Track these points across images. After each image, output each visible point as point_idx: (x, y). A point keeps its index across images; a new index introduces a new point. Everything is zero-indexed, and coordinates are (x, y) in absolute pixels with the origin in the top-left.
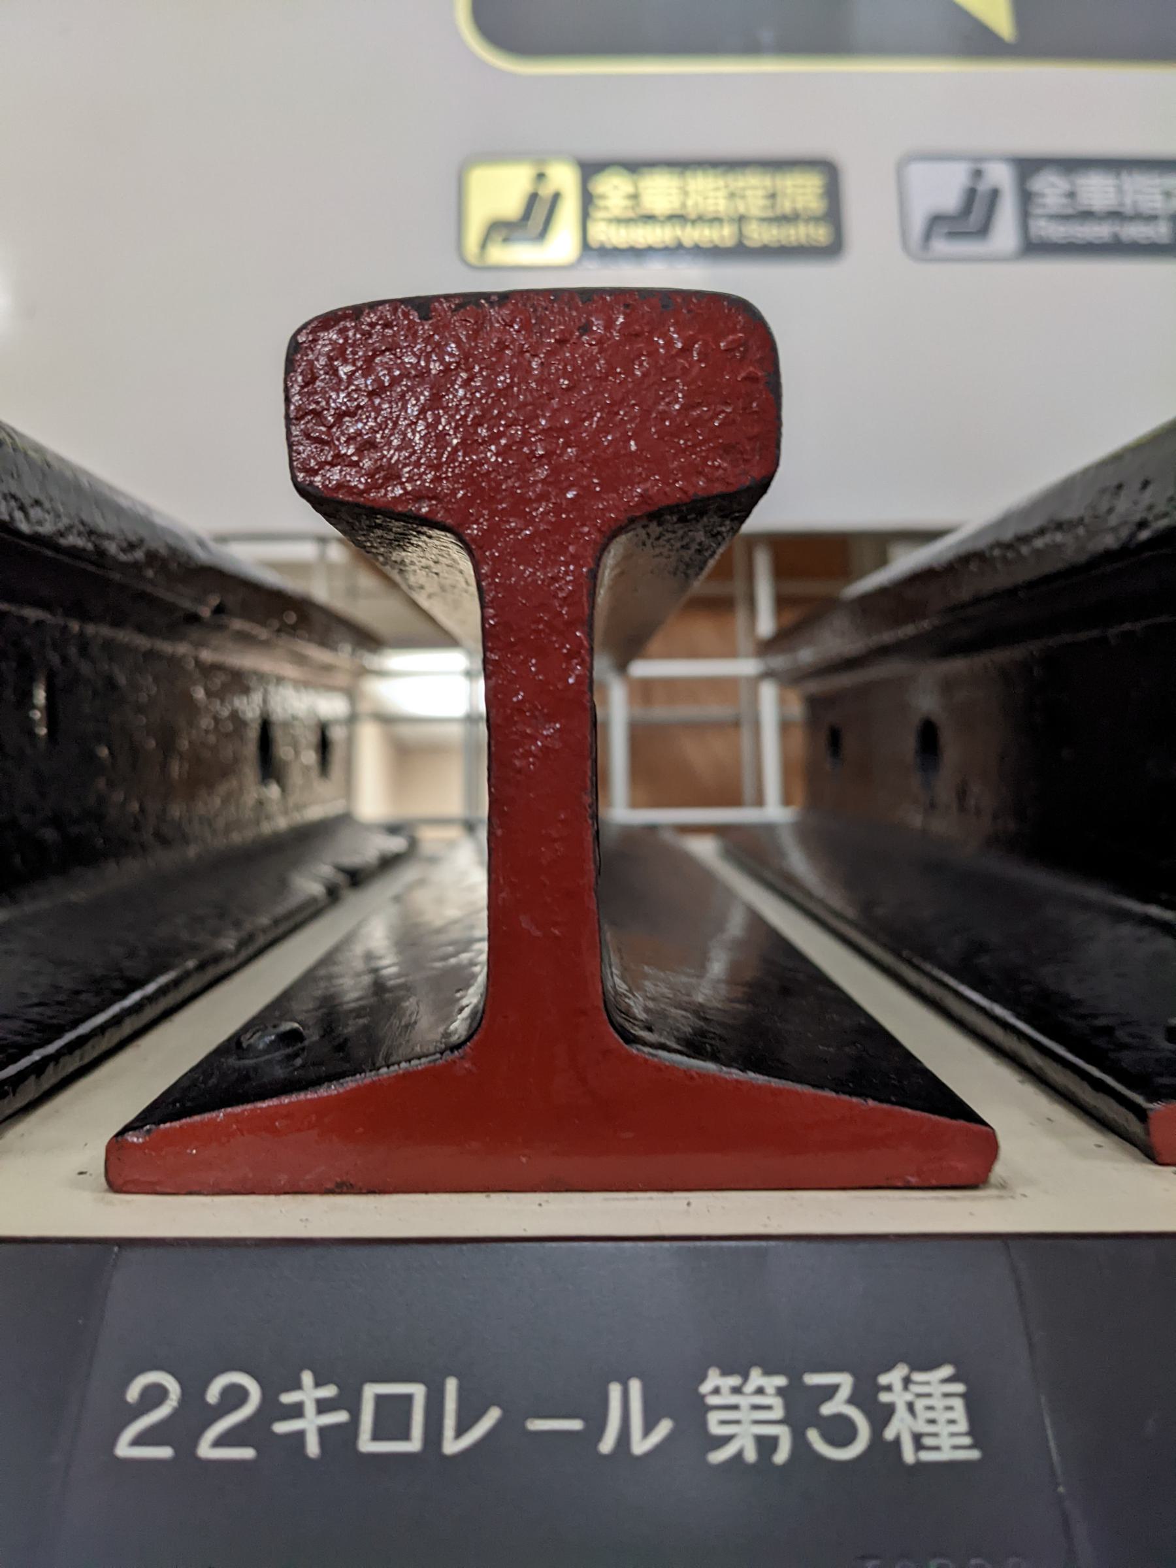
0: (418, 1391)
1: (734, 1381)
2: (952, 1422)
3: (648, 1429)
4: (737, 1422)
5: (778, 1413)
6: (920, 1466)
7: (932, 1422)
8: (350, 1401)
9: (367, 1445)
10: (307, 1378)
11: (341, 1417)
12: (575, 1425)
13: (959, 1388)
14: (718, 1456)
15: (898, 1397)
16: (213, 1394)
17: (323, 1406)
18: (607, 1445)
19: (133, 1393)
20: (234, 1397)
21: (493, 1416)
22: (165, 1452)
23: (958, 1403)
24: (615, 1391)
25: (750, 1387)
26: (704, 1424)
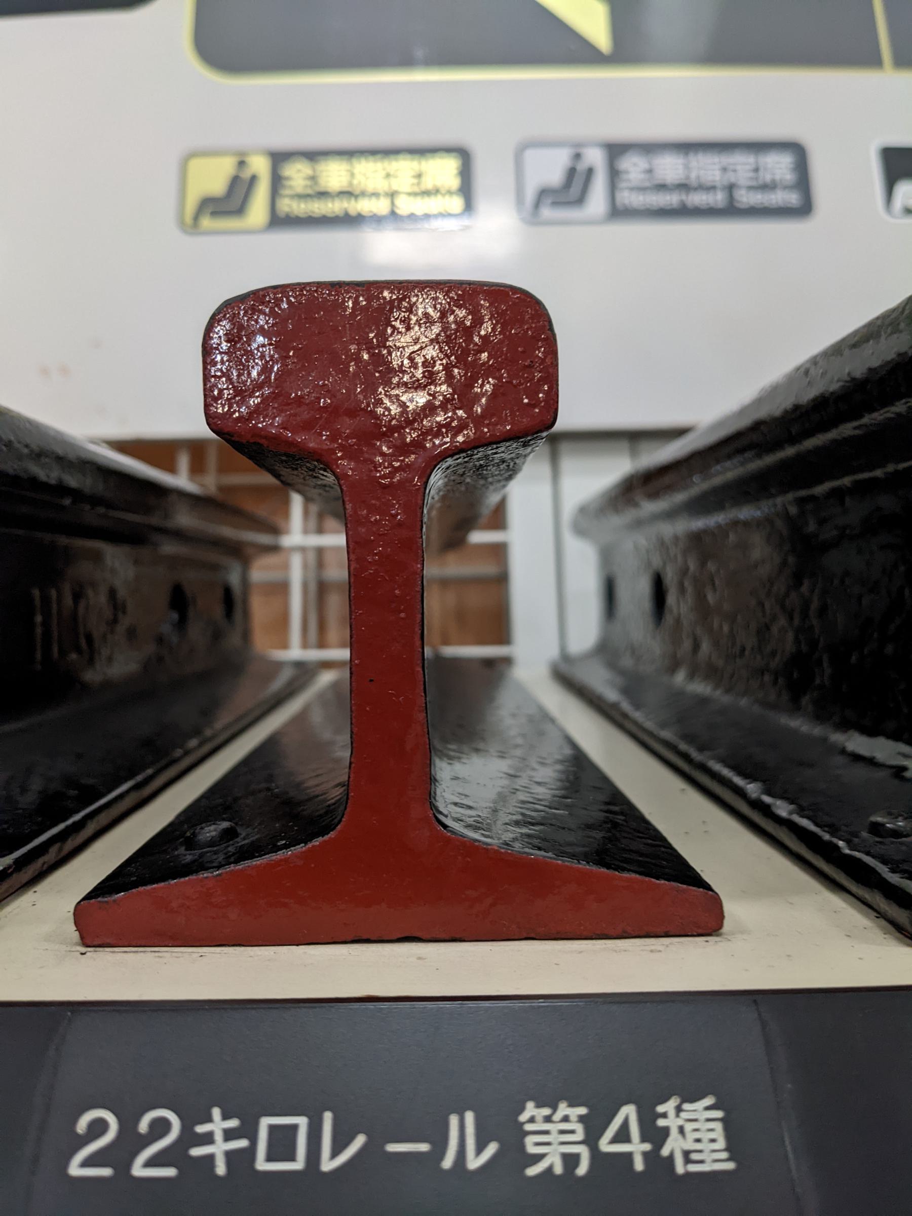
0: (302, 1122)
1: (546, 1111)
2: (713, 1141)
3: (480, 1149)
5: (580, 1136)
6: (688, 1175)
7: (698, 1141)
8: (248, 1131)
9: (262, 1165)
10: (216, 1112)
11: (243, 1143)
12: (424, 1147)
13: (719, 1114)
15: (671, 1122)
16: (143, 1126)
17: (229, 1135)
18: (448, 1163)
19: (82, 1124)
20: (160, 1128)
21: (360, 1141)
22: (106, 1172)
23: (718, 1126)
24: (454, 1120)
25: (558, 1116)
26: (522, 1147)
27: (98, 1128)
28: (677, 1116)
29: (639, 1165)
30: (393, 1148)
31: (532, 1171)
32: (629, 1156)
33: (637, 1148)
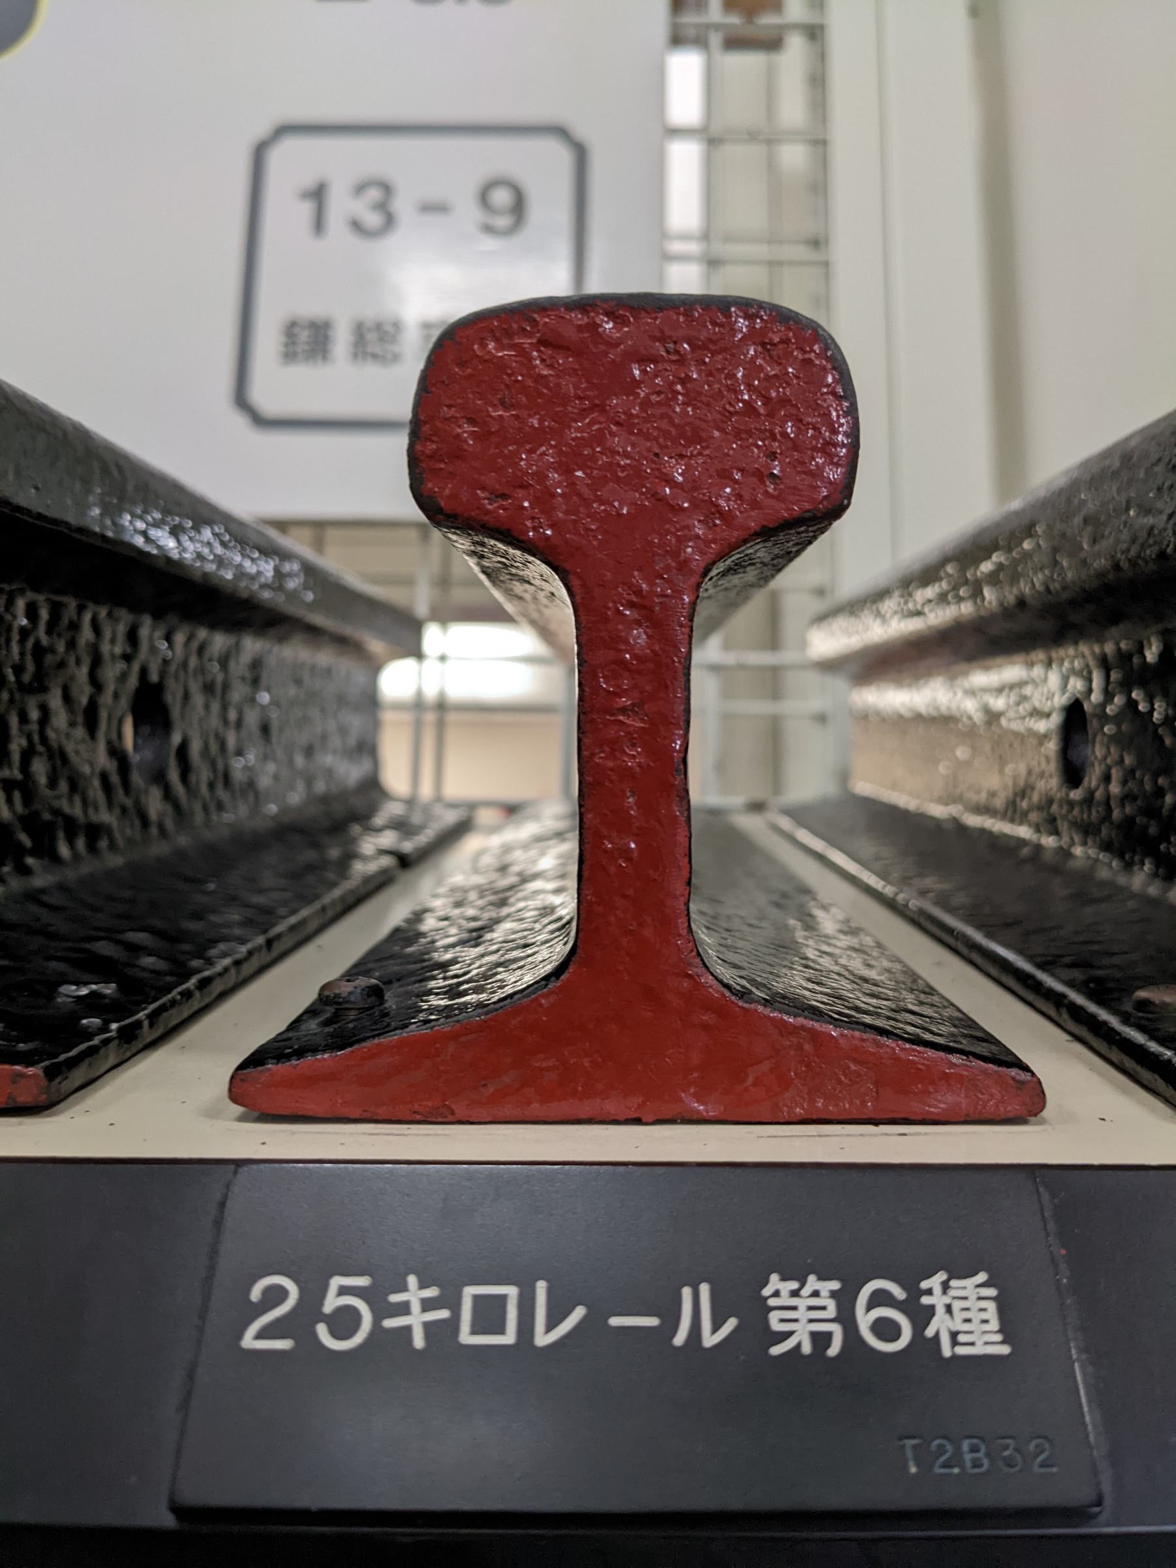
0: (512, 1291)
1: (794, 1285)
2: (985, 1321)
4: (796, 1320)
5: (831, 1312)
6: (955, 1357)
7: (968, 1321)
9: (466, 1337)
10: (412, 1280)
11: (444, 1314)
12: (652, 1322)
13: (992, 1292)
15: (937, 1300)
17: (427, 1305)
18: (680, 1339)
21: (579, 1313)
23: (991, 1306)
24: (687, 1292)
25: (806, 1291)
27: (276, 1295)
30: (615, 1321)
31: (776, 1350)
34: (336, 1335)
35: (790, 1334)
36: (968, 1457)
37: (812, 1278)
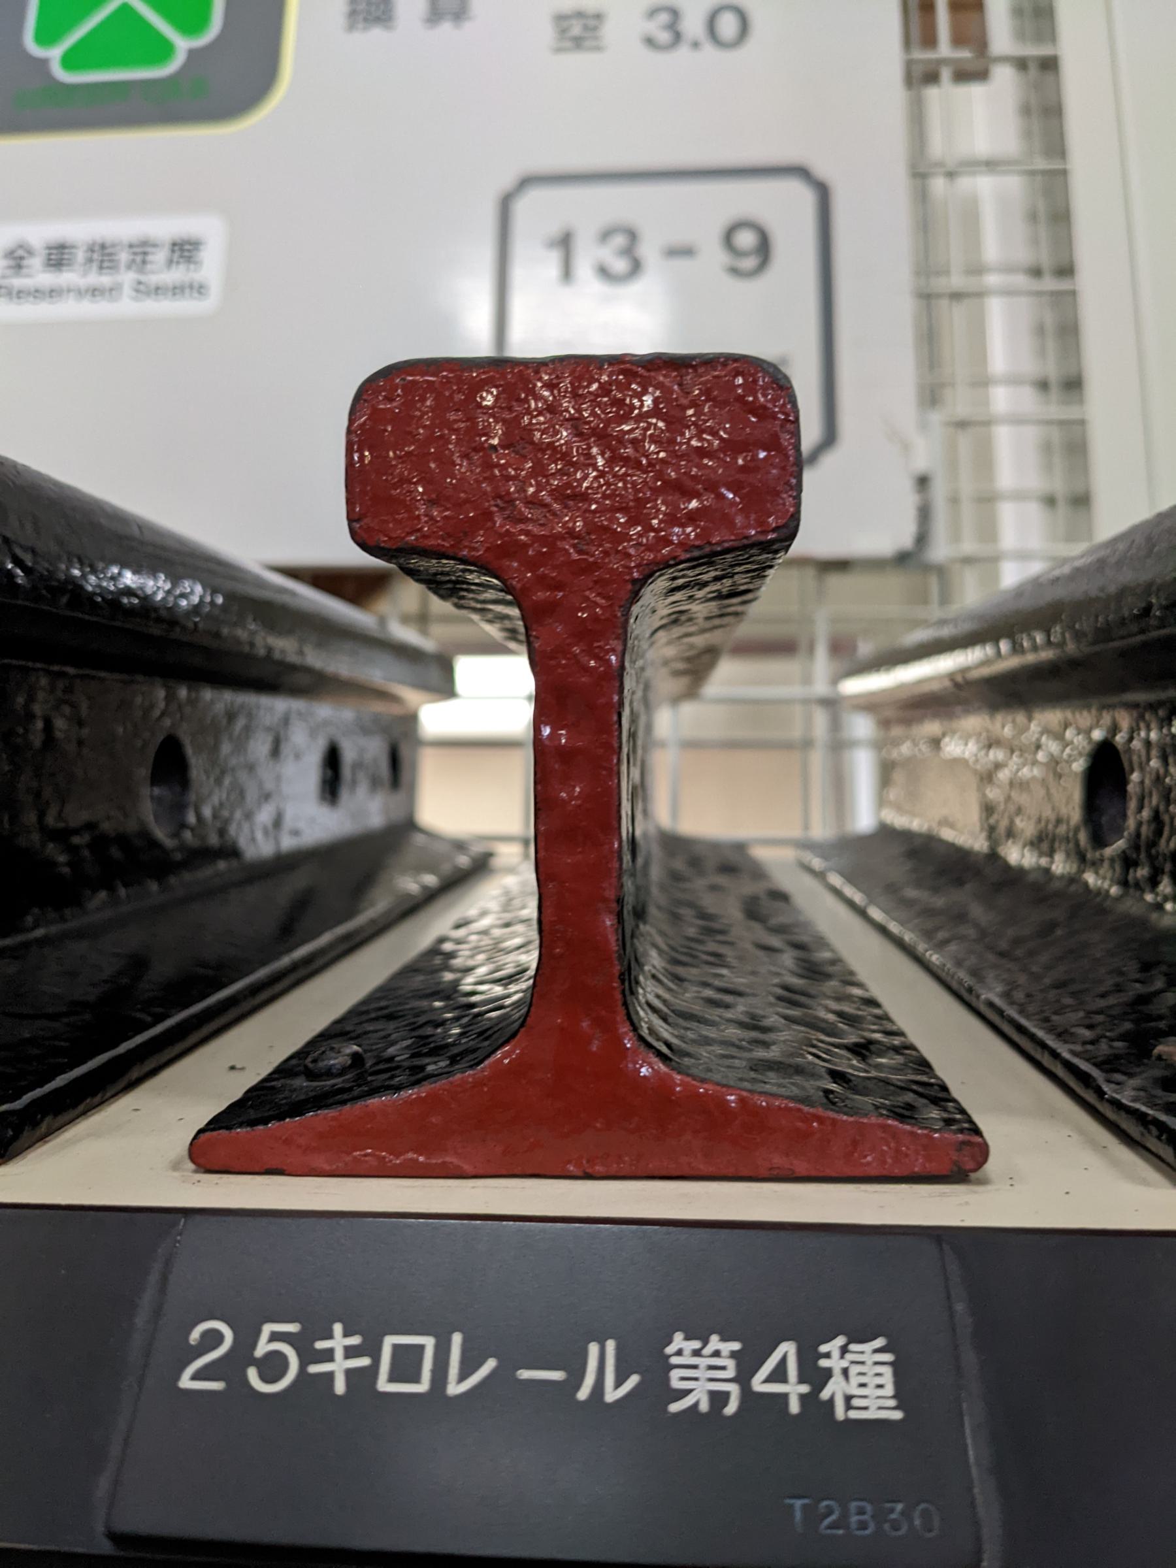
0: (429, 1342)
1: (696, 1344)
2: (880, 1386)
4: (696, 1379)
5: (730, 1373)
6: (848, 1421)
7: (863, 1385)
8: (371, 1348)
9: (384, 1385)
10: (338, 1328)
11: (365, 1362)
13: (888, 1357)
14: (675, 1407)
15: (834, 1363)
17: (350, 1352)
19: (195, 1335)
21: (491, 1364)
23: (887, 1371)
24: (593, 1349)
25: (708, 1350)
26: (668, 1379)
27: (213, 1339)
28: (842, 1357)
29: (794, 1407)
30: (525, 1374)
32: (784, 1397)
33: (794, 1390)
34: (267, 1379)
35: (689, 1391)
36: (854, 1519)
37: (714, 1338)
